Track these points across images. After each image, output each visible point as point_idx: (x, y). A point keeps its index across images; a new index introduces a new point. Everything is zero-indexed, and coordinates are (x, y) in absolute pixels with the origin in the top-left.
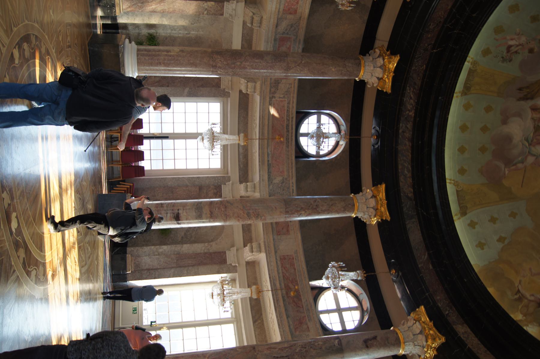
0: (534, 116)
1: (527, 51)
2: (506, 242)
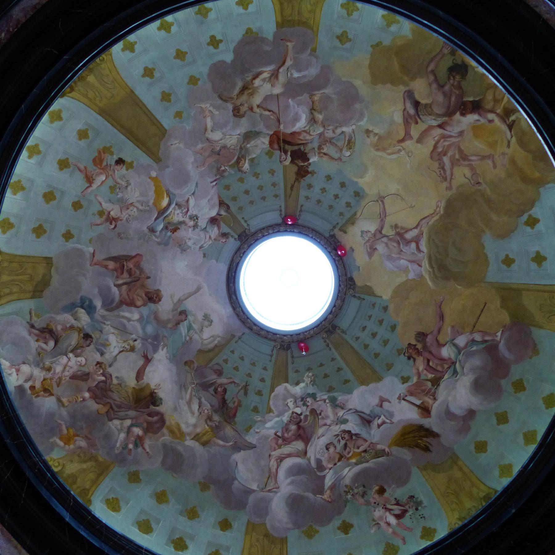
0: (430, 402)
1: (386, 495)
2: (525, 217)
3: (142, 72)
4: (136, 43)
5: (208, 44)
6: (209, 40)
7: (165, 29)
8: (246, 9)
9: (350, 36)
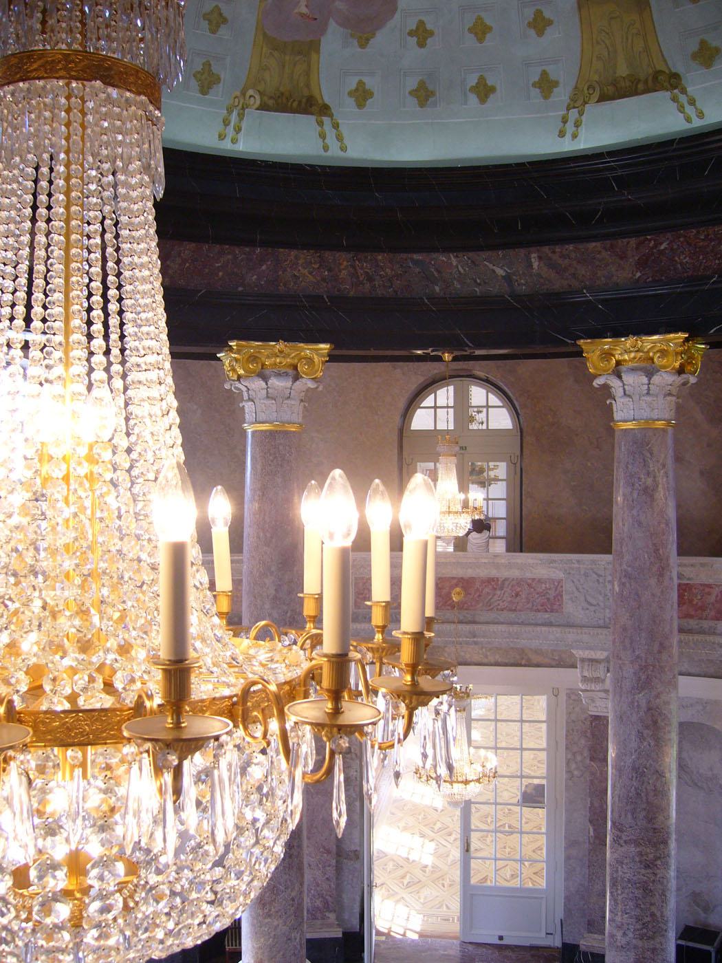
3: (549, 30)
4: (534, 85)
5: (431, 34)
6: (429, 41)
7: (486, 85)
8: (361, 83)
9: (205, 24)
